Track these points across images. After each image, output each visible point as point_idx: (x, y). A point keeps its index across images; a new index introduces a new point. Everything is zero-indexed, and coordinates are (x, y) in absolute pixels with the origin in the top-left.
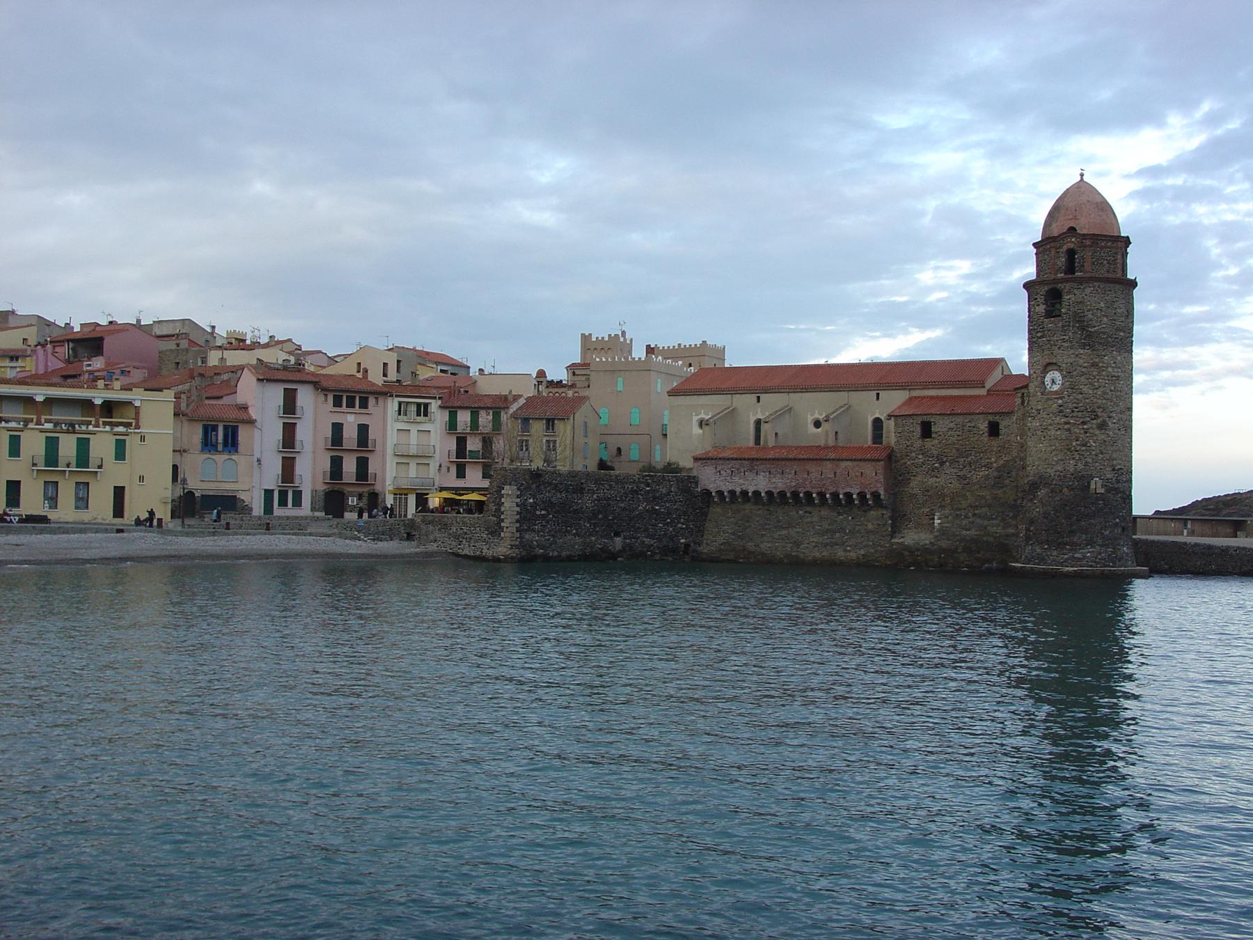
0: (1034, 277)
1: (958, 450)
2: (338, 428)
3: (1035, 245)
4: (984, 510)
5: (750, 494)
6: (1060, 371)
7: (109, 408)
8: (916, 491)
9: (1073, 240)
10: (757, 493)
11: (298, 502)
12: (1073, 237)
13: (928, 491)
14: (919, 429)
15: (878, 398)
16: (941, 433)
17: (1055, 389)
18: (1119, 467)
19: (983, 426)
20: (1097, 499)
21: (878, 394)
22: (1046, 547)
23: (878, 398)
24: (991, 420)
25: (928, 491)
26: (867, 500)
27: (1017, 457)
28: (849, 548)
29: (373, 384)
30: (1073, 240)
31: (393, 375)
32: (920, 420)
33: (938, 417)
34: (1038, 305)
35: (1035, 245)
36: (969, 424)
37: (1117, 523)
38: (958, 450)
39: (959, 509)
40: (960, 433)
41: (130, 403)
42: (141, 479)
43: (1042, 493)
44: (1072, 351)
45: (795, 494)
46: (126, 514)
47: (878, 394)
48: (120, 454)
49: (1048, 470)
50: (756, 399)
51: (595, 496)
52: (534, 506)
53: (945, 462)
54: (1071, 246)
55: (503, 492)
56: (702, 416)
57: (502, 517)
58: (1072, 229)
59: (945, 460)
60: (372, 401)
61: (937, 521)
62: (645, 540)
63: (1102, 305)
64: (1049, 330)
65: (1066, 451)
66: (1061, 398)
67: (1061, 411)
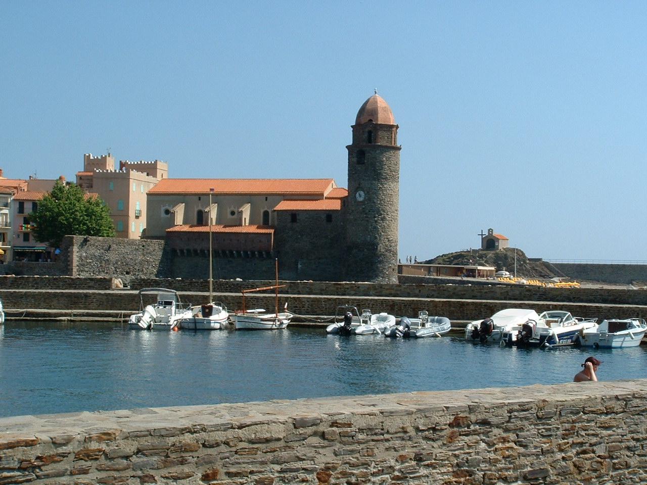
3: (352, 126)
5: (199, 251)
6: (363, 191)
9: (371, 126)
14: (289, 218)
15: (266, 200)
17: (361, 200)
18: (391, 239)
19: (324, 217)
20: (381, 255)
21: (266, 198)
23: (266, 200)
26: (263, 255)
35: (352, 126)
37: (390, 267)
47: (266, 198)
49: (358, 240)
50: (198, 198)
52: (86, 258)
54: (370, 129)
55: (69, 250)
56: (167, 207)
57: (69, 263)
61: (300, 266)
63: (384, 159)
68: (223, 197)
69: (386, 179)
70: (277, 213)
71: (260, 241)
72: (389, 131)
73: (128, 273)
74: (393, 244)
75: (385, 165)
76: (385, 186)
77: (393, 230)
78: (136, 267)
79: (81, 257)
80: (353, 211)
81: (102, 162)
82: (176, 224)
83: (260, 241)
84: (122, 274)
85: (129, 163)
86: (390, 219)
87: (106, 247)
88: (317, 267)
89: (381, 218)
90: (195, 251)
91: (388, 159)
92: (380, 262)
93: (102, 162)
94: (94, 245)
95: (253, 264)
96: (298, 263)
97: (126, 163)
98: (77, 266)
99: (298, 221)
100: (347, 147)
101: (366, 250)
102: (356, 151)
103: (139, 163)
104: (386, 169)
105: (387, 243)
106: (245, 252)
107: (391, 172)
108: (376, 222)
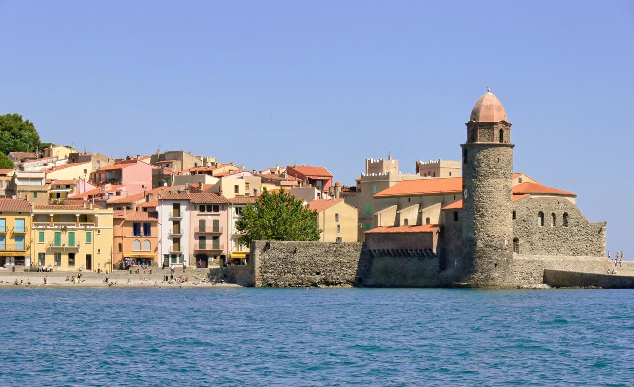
0: (466, 143)
2: (202, 223)
7: (85, 218)
8: (452, 248)
10: (388, 251)
11: (182, 260)
14: (452, 216)
18: (492, 234)
20: (480, 250)
29: (224, 198)
31: (242, 191)
37: (491, 262)
41: (92, 215)
42: (99, 251)
46: (92, 268)
48: (89, 240)
50: (408, 200)
51: (304, 254)
52: (270, 260)
60: (220, 207)
61: (455, 263)
62: (333, 276)
63: (482, 157)
68: (425, 197)
69: (484, 176)
70: (445, 211)
71: (425, 241)
72: (490, 128)
73: (318, 273)
74: (496, 240)
75: (483, 162)
76: (484, 183)
77: (494, 226)
78: (327, 267)
79: (264, 260)
81: (376, 167)
82: (379, 225)
84: (311, 274)
85: (422, 163)
86: (490, 215)
87: (292, 249)
89: (479, 215)
90: (384, 251)
91: (486, 156)
92: (480, 257)
93: (376, 167)
94: (278, 249)
97: (420, 163)
98: (260, 267)
99: (458, 219)
100: (461, 145)
103: (428, 162)
104: (484, 168)
105: (487, 239)
106: (416, 251)
107: (490, 168)
108: (475, 218)
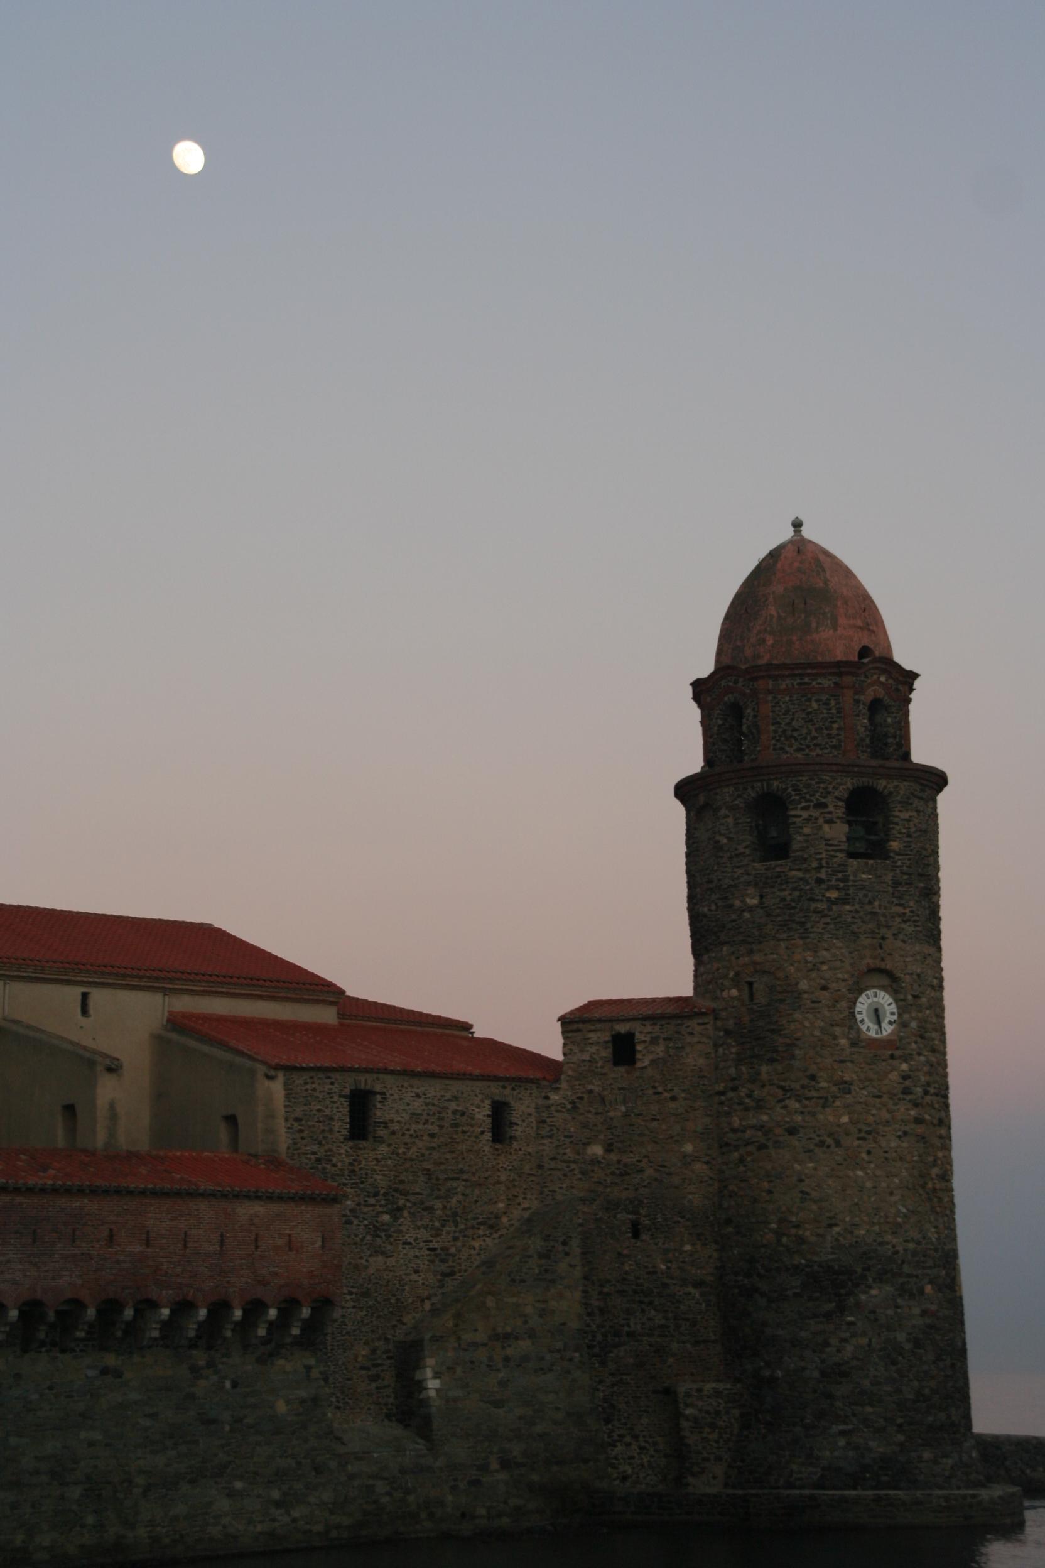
1: (428, 1173)
4: (525, 1345)
12: (884, 671)
13: (366, 1294)
14: (345, 1109)
15: (85, 1011)
16: (396, 1127)
19: (482, 1114)
21: (85, 996)
22: (901, 1438)
23: (85, 1011)
24: (497, 1098)
25: (366, 1294)
27: (583, 1200)
28: (238, 1485)
30: (883, 679)
32: (347, 1083)
33: (390, 1079)
34: (830, 822)
36: (453, 1106)
38: (428, 1173)
39: (474, 1345)
40: (436, 1130)
43: (876, 1294)
44: (917, 948)
45: (110, 1308)
47: (85, 996)
49: (888, 1237)
53: (399, 1209)
54: (881, 693)
58: (865, 652)
59: (401, 1202)
61: (433, 1384)
64: (863, 888)
65: (921, 1191)
66: (906, 1059)
67: (907, 1091)
71: (290, 1245)
80: (845, 1087)
83: (290, 1245)
88: (503, 1384)
95: (228, 1384)
96: (418, 1365)
101: (928, 1289)
102: (843, 791)
